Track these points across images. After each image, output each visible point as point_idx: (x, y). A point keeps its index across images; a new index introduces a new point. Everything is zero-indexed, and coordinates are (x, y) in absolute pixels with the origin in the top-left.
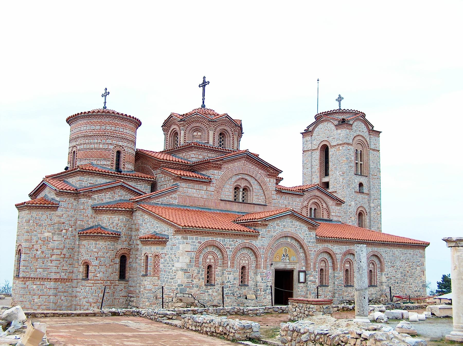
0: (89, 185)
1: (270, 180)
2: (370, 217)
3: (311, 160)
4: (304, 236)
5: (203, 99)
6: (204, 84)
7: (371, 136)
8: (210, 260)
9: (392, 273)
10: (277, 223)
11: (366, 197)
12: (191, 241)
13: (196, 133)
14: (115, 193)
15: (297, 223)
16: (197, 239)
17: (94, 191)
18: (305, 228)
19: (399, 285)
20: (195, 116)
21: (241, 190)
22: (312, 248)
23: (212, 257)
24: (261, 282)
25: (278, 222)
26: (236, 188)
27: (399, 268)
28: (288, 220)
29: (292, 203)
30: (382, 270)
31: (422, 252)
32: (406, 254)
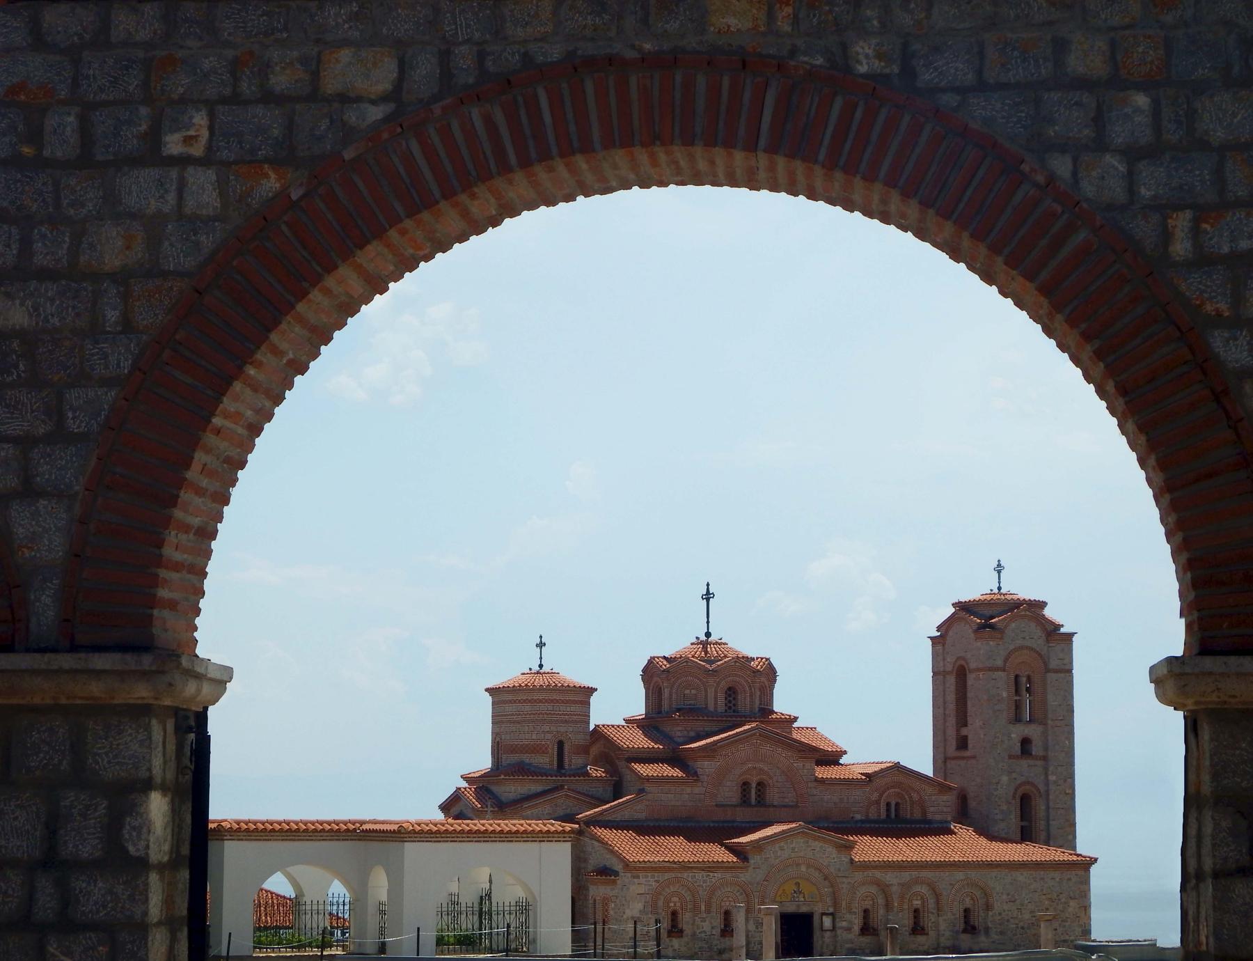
0: (519, 797)
1: (804, 765)
2: (1048, 800)
3: (944, 691)
4: (830, 862)
5: (708, 622)
6: (708, 596)
7: (1051, 645)
8: (675, 903)
9: (1010, 913)
10: (780, 847)
11: (1040, 763)
12: (645, 880)
13: (689, 691)
14: (556, 805)
15: (817, 845)
16: (653, 877)
17: (526, 807)
18: (831, 849)
19: (1026, 933)
20: (685, 664)
21: (754, 785)
22: (844, 880)
23: (678, 899)
24: (755, 931)
25: (782, 844)
26: (745, 785)
27: (1026, 902)
28: (799, 840)
29: (848, 798)
30: (988, 907)
31: (1083, 874)
32: (1043, 879)
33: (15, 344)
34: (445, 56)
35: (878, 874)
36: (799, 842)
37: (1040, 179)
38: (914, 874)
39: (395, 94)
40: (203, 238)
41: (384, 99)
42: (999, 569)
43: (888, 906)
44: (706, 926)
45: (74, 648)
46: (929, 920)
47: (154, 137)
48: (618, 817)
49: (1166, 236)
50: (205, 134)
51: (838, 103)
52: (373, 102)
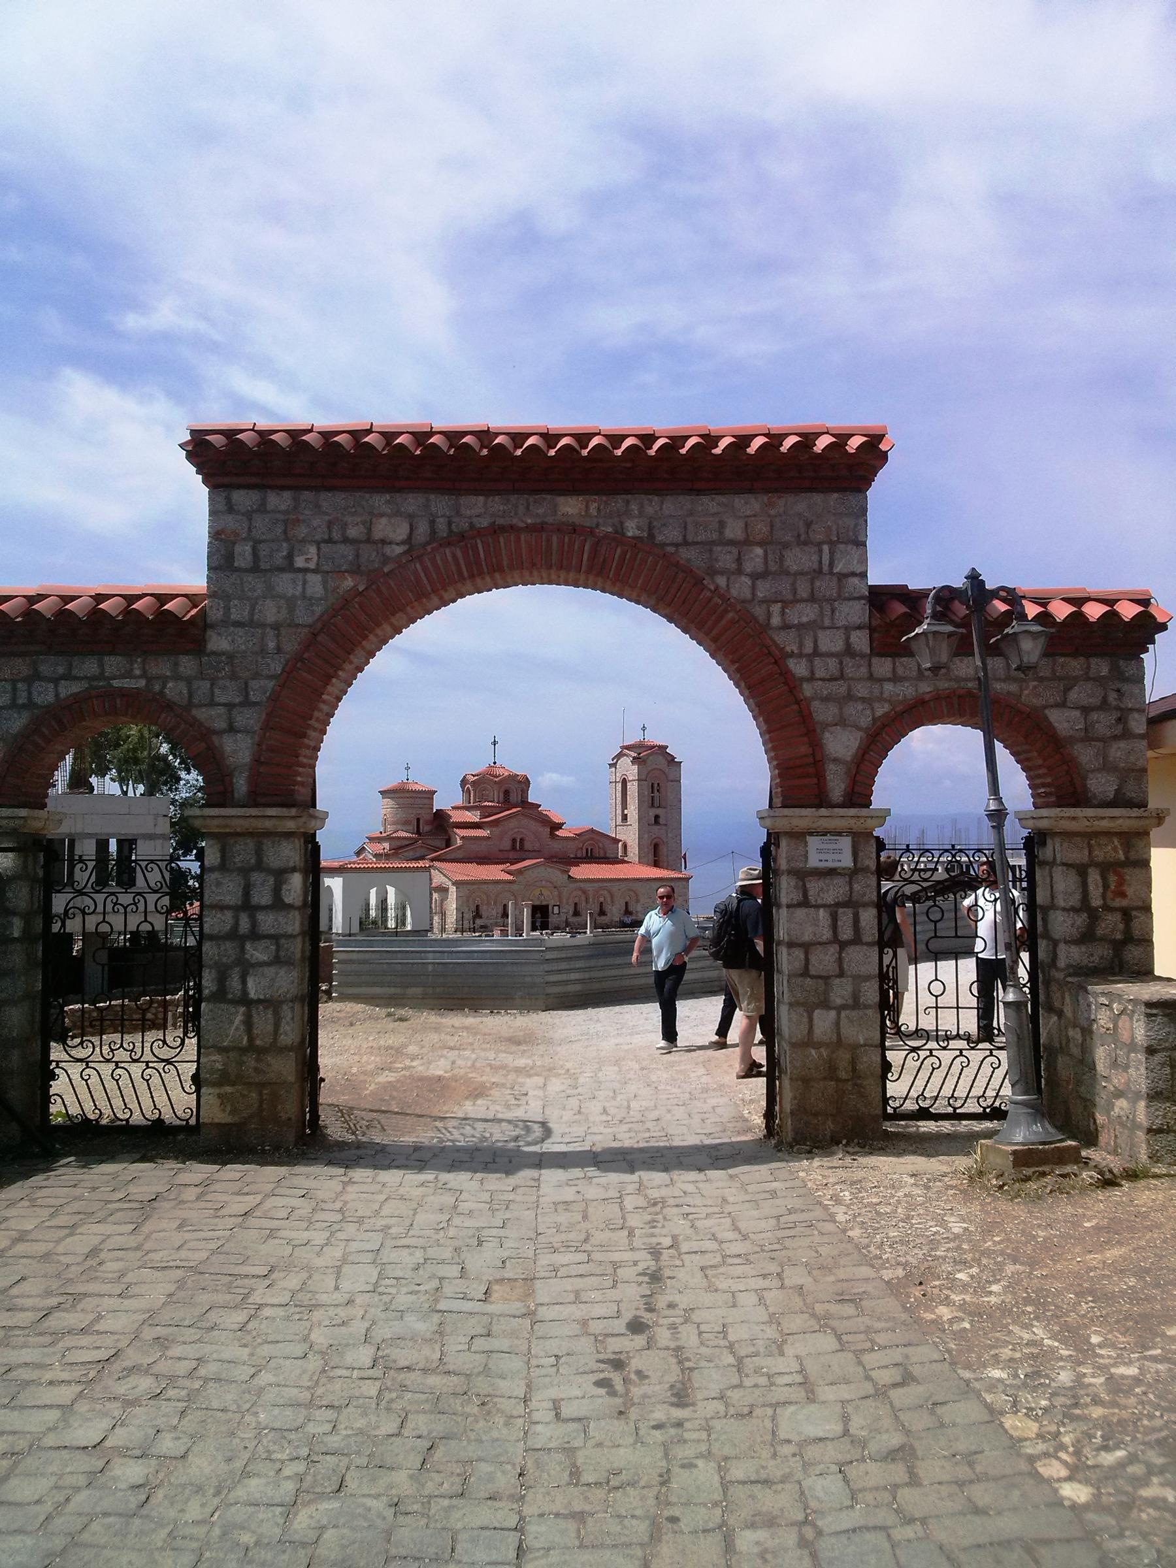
6: (495, 743)
15: (549, 870)
26: (514, 840)
30: (638, 901)
33: (223, 658)
34: (432, 523)
35: (582, 885)
36: (542, 869)
37: (712, 588)
38: (600, 884)
39: (408, 541)
40: (315, 608)
41: (403, 543)
42: (644, 729)
43: (587, 901)
44: (494, 912)
45: (256, 805)
46: (607, 908)
47: (290, 557)
48: (448, 857)
49: (769, 615)
50: (315, 558)
51: (619, 551)
52: (397, 544)
